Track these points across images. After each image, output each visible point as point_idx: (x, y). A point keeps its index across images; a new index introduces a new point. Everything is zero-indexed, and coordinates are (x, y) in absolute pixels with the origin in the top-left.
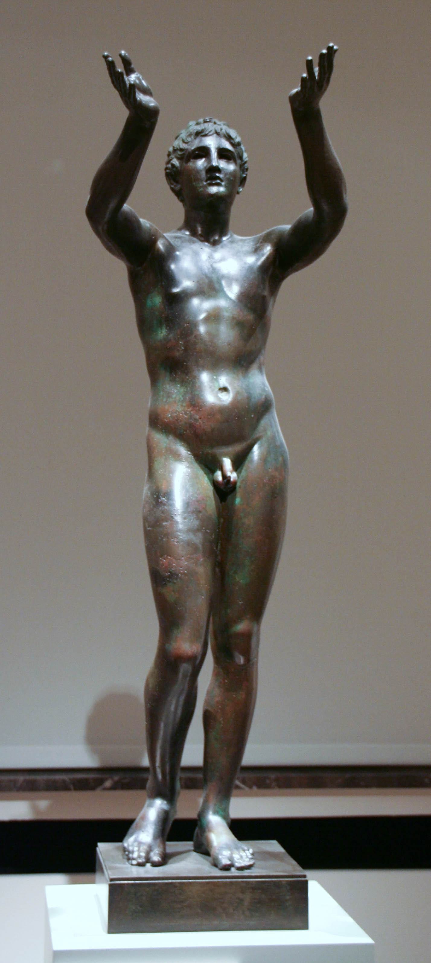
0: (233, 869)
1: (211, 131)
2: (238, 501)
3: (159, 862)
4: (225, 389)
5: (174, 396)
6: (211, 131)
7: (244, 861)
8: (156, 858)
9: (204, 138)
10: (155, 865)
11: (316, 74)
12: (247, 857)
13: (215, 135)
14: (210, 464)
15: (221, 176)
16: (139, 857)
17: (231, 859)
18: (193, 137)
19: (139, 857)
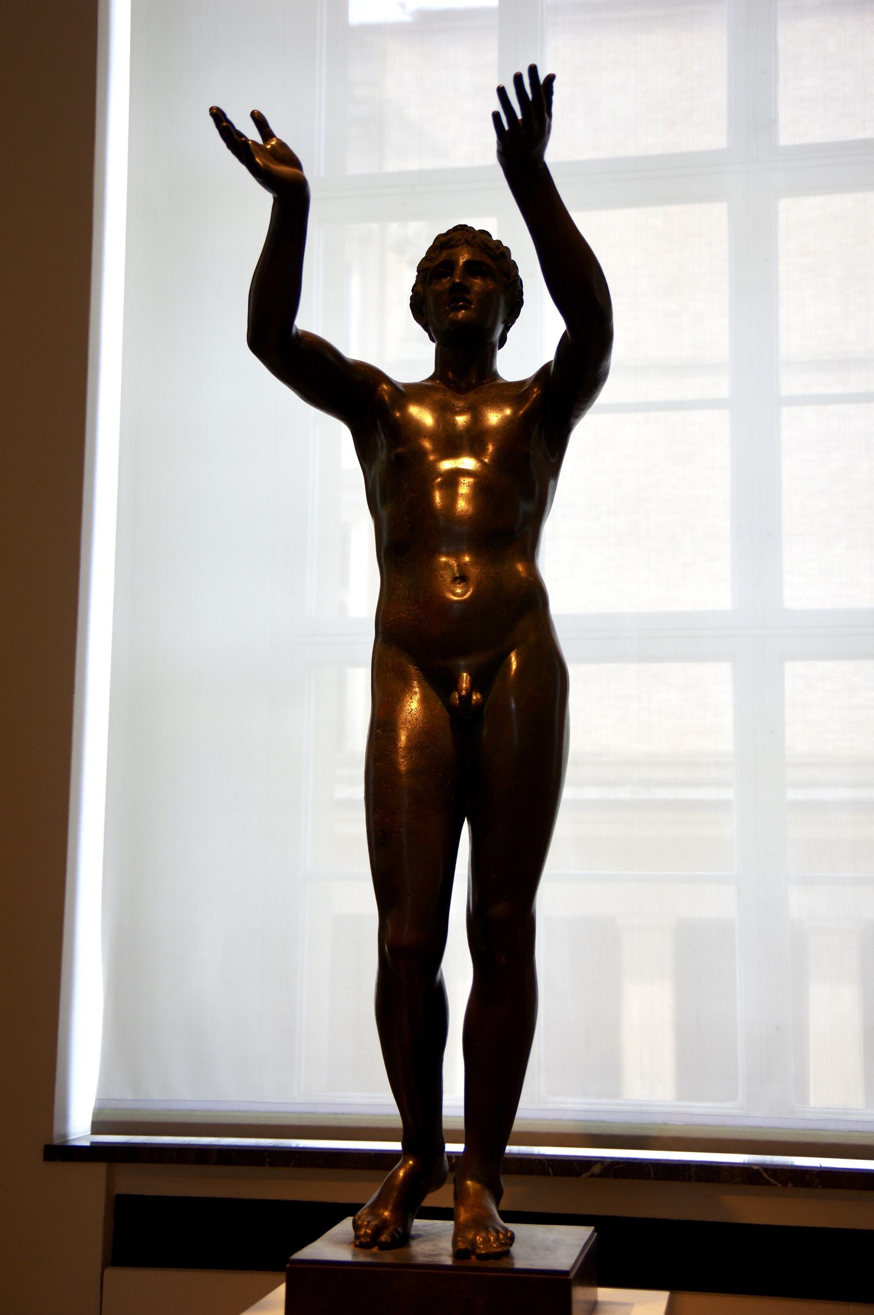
0: (473, 1257)
1: (460, 240)
2: (485, 732)
3: (386, 1243)
4: (462, 578)
5: (398, 592)
6: (460, 240)
7: (492, 1246)
8: (384, 1238)
9: (453, 251)
10: (384, 1247)
11: (507, 128)
12: (497, 1239)
13: (466, 245)
14: (440, 683)
15: (472, 297)
16: (366, 1233)
17: (473, 1243)
18: (437, 252)
19: (366, 1233)
